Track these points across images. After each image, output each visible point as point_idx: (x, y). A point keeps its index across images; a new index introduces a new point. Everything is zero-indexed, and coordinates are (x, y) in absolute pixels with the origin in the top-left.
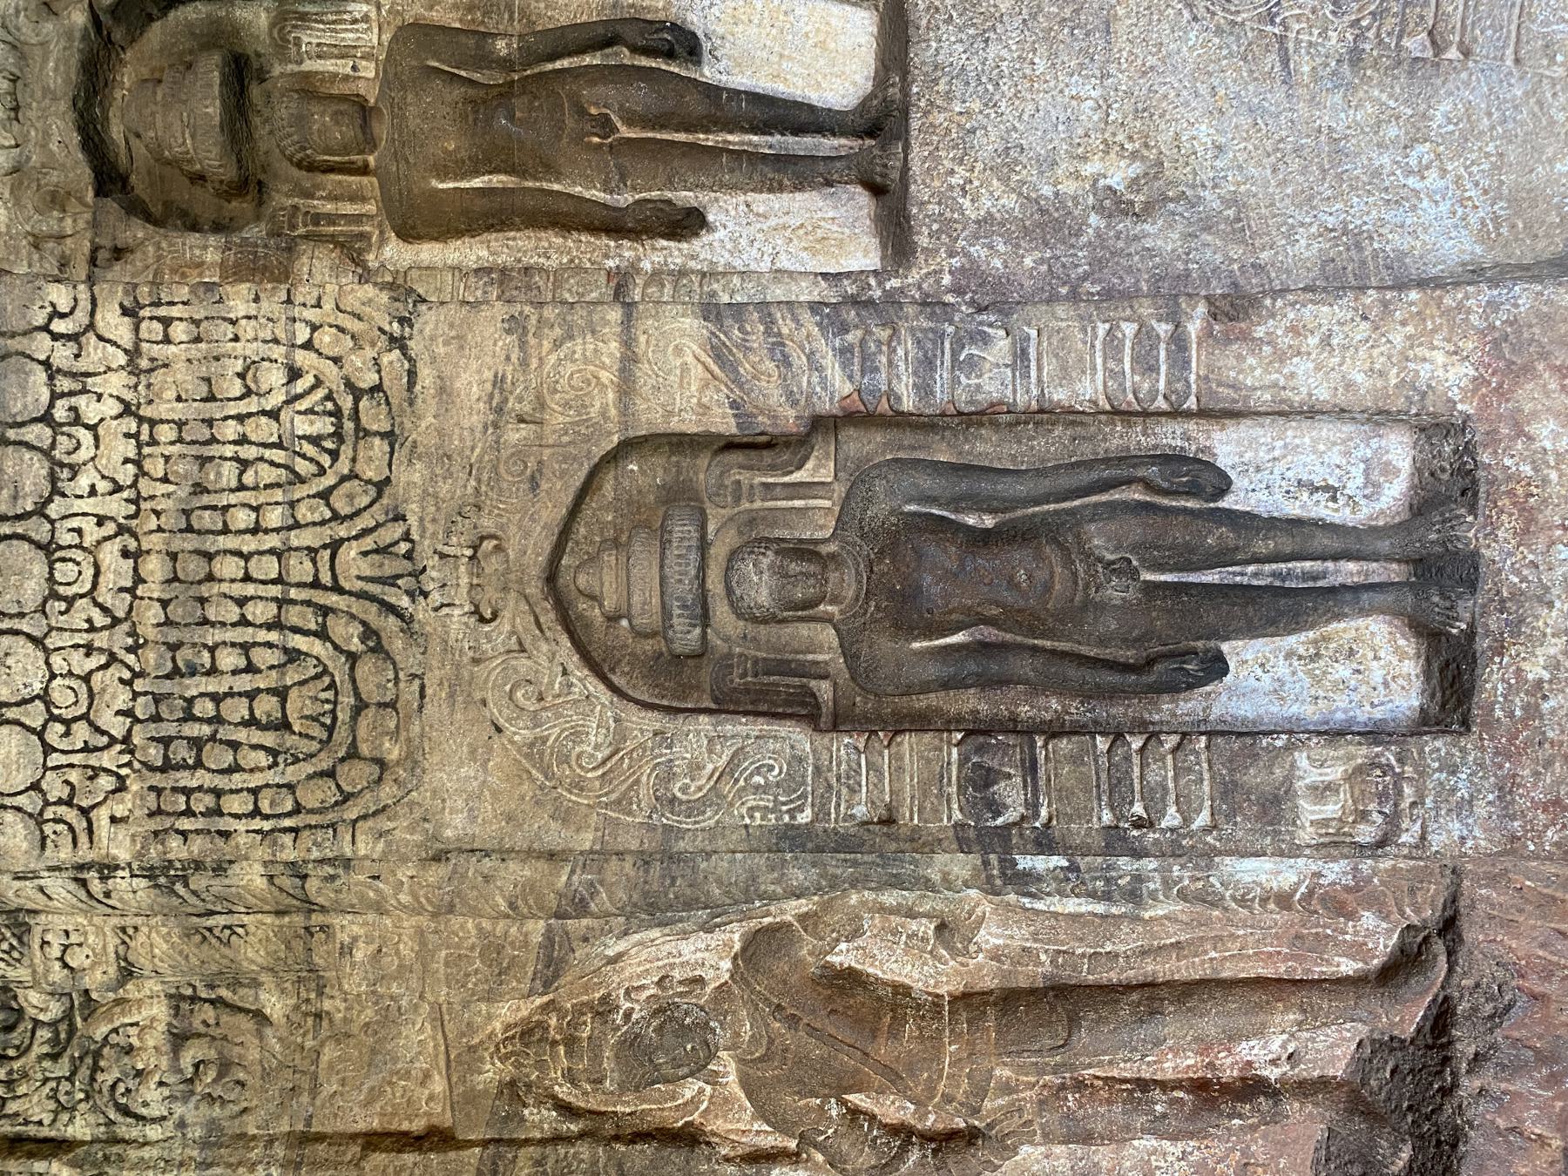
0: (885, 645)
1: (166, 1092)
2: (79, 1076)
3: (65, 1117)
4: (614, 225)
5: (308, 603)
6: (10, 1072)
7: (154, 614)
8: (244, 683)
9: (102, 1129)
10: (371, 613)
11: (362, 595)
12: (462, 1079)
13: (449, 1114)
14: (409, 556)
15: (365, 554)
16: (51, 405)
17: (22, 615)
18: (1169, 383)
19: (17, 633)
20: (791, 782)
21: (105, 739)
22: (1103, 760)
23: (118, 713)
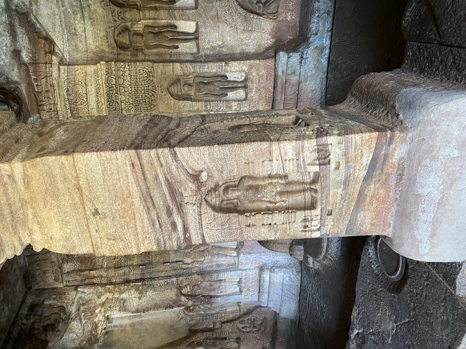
0: (197, 93)
4: (169, 48)
7: (134, 93)
10: (152, 92)
20: (190, 106)
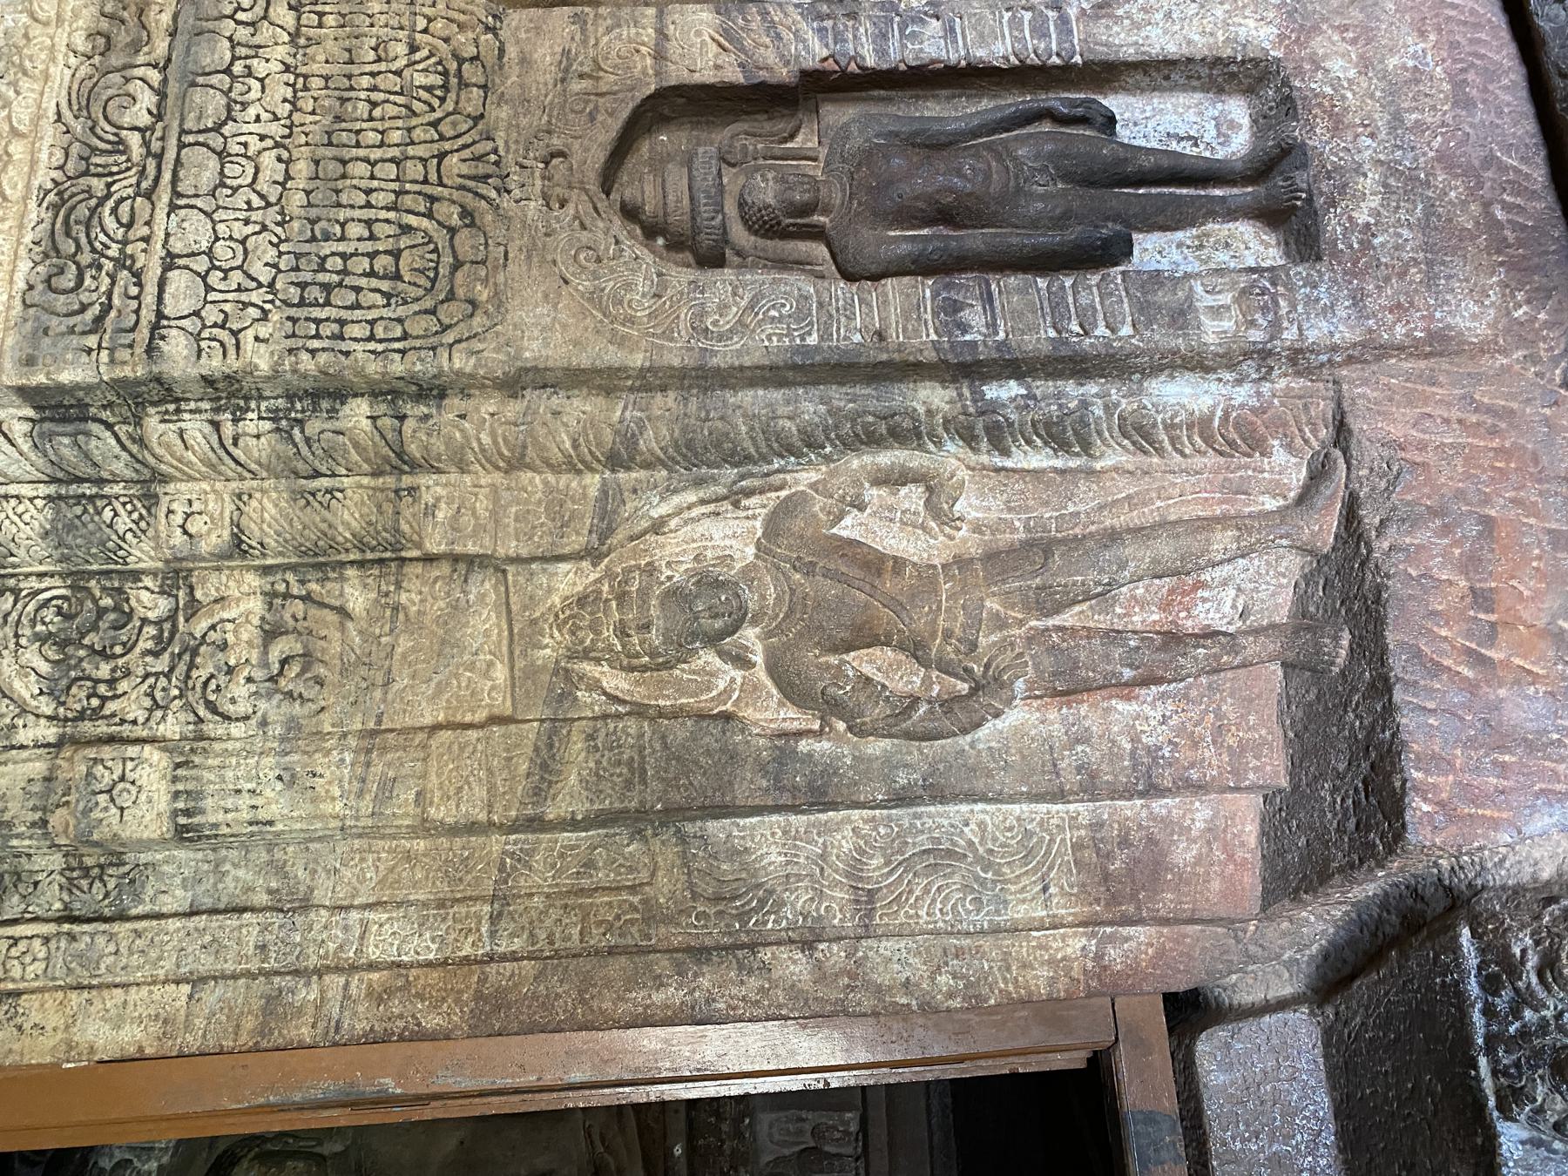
1: (253, 688)
2: (177, 672)
3: (159, 713)
5: (419, 193)
6: (113, 670)
7: (299, 198)
8: (368, 247)
9: (191, 727)
11: (462, 188)
12: (524, 654)
13: (509, 703)
14: (497, 164)
15: (464, 161)
16: (231, 64)
17: (197, 196)
18: (1059, 44)
19: (192, 207)
20: (801, 315)
21: (254, 284)
22: (1044, 293)
23: (267, 264)
